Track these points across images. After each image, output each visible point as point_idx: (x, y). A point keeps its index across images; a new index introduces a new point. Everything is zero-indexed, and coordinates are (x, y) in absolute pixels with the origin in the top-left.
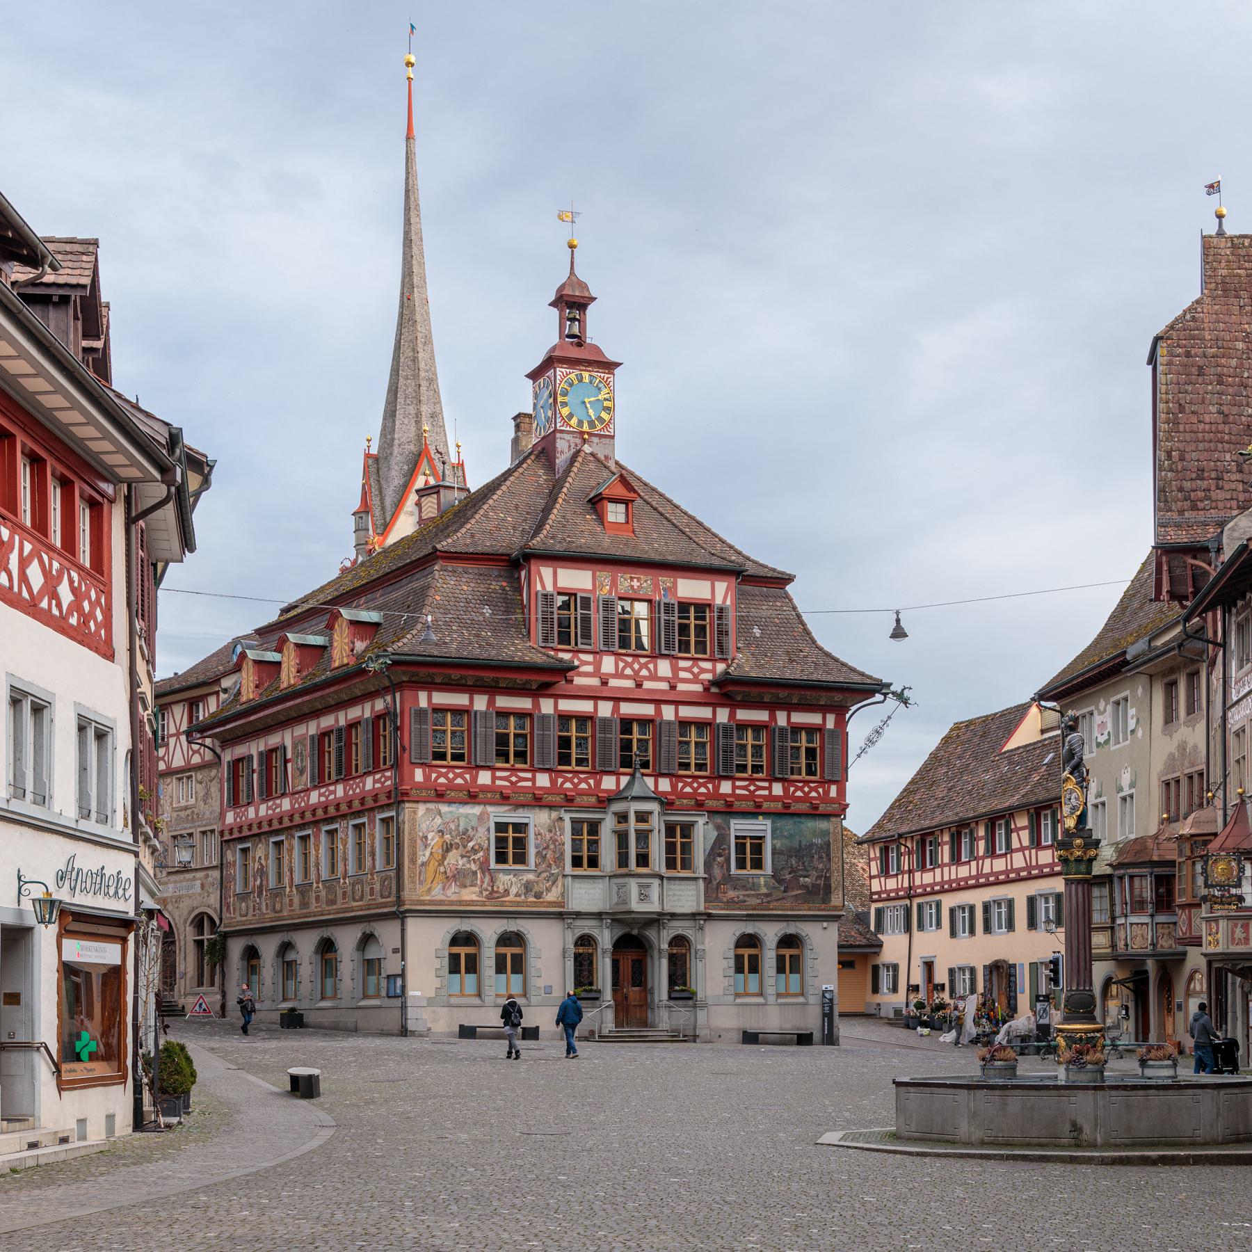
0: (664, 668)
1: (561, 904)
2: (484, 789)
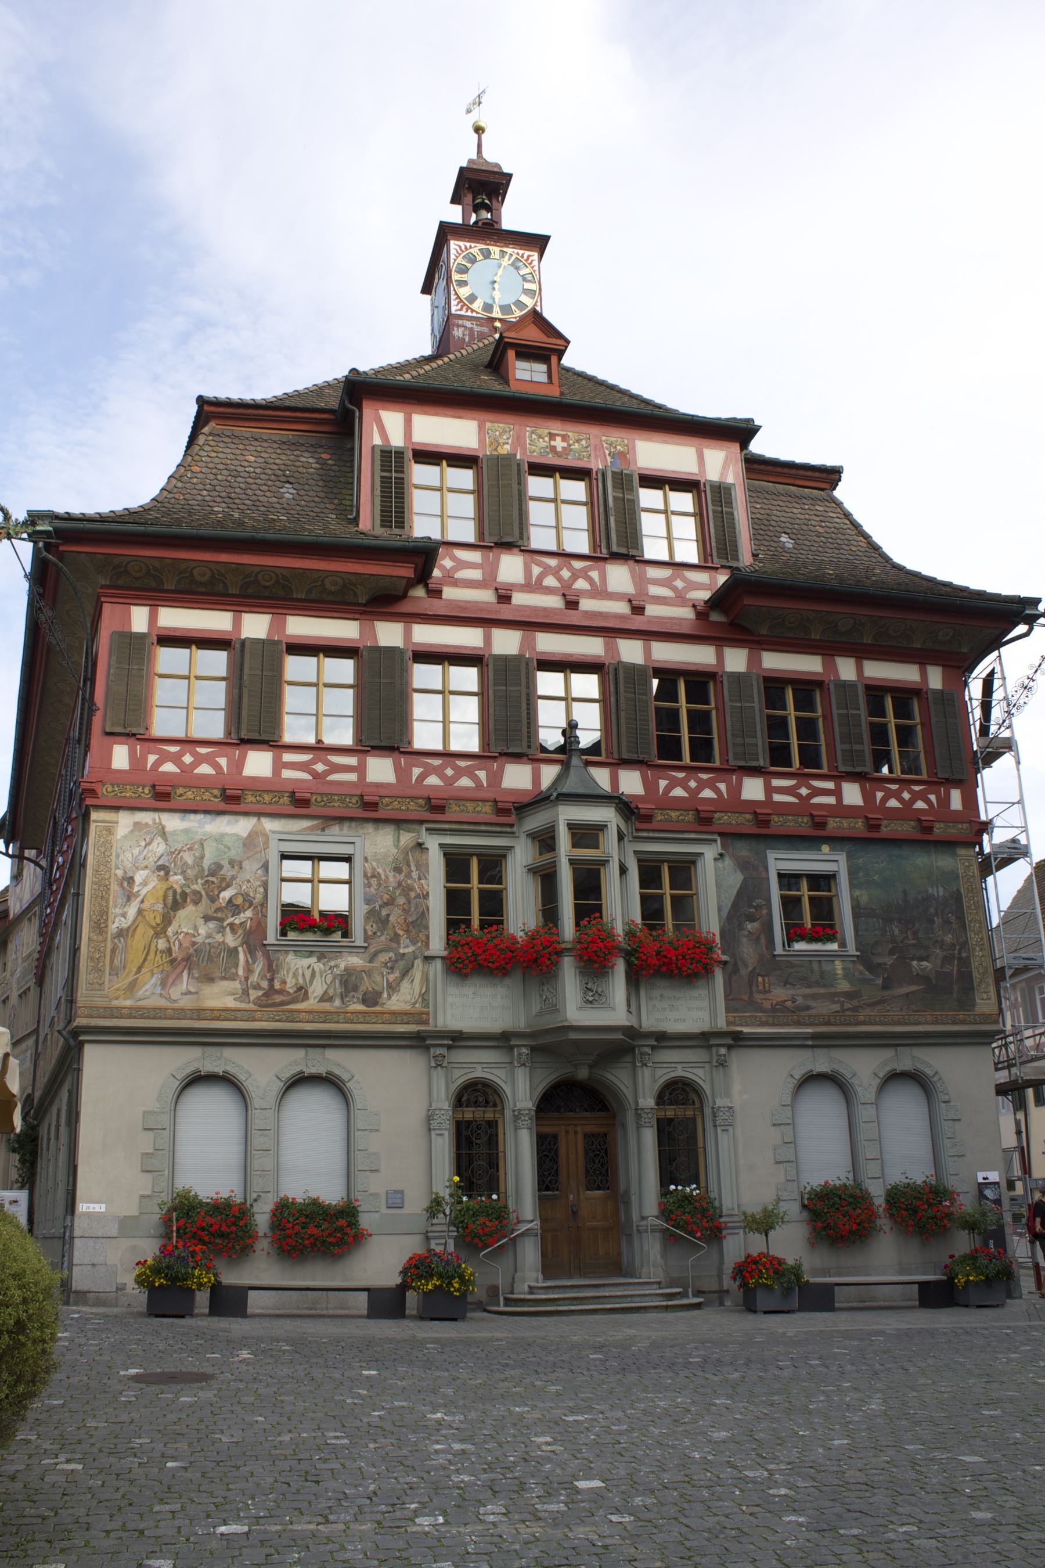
1: (420, 1017)
2: (257, 786)
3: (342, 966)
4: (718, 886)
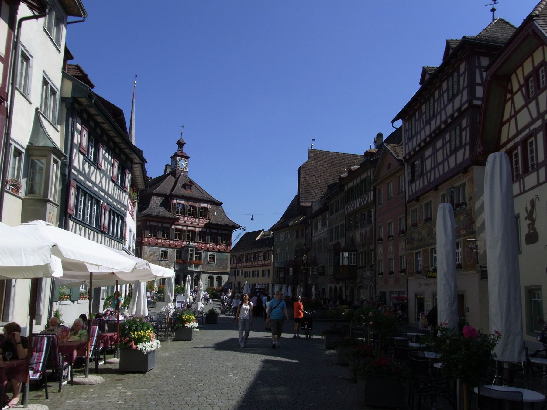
0: (197, 220)
2: (159, 243)
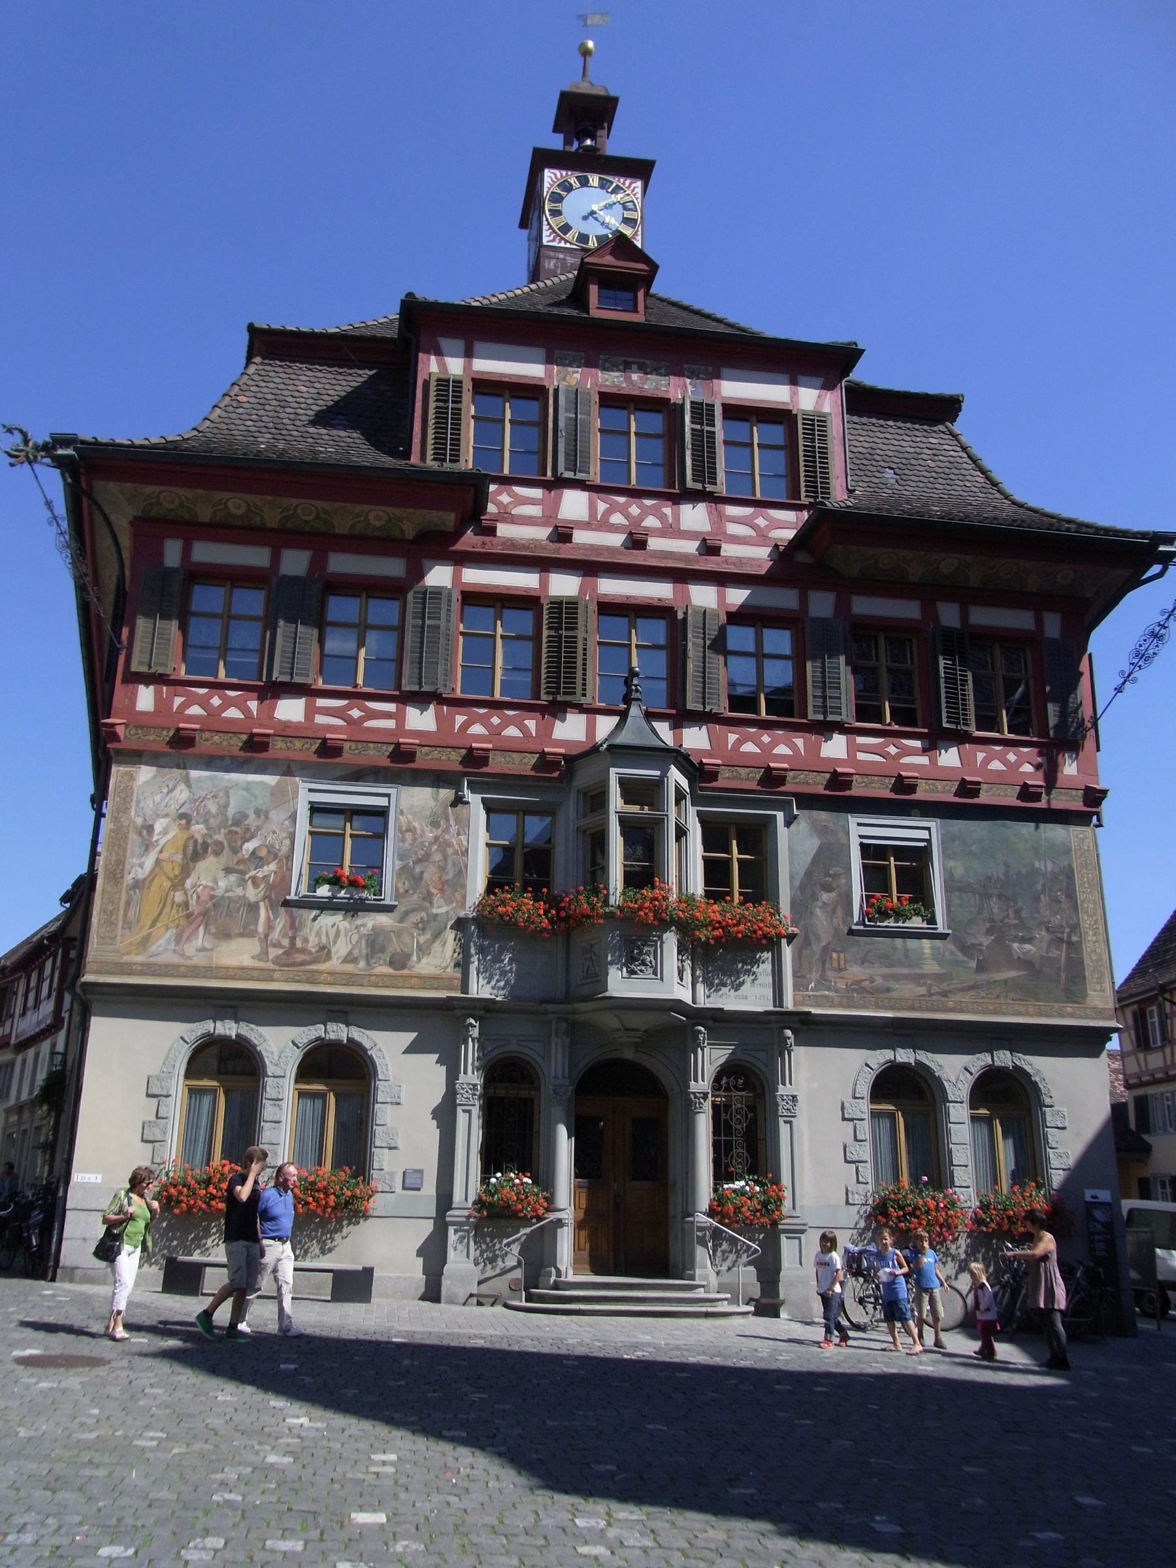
0: (695, 516)
2: (287, 731)
3: (370, 925)
4: (791, 850)
